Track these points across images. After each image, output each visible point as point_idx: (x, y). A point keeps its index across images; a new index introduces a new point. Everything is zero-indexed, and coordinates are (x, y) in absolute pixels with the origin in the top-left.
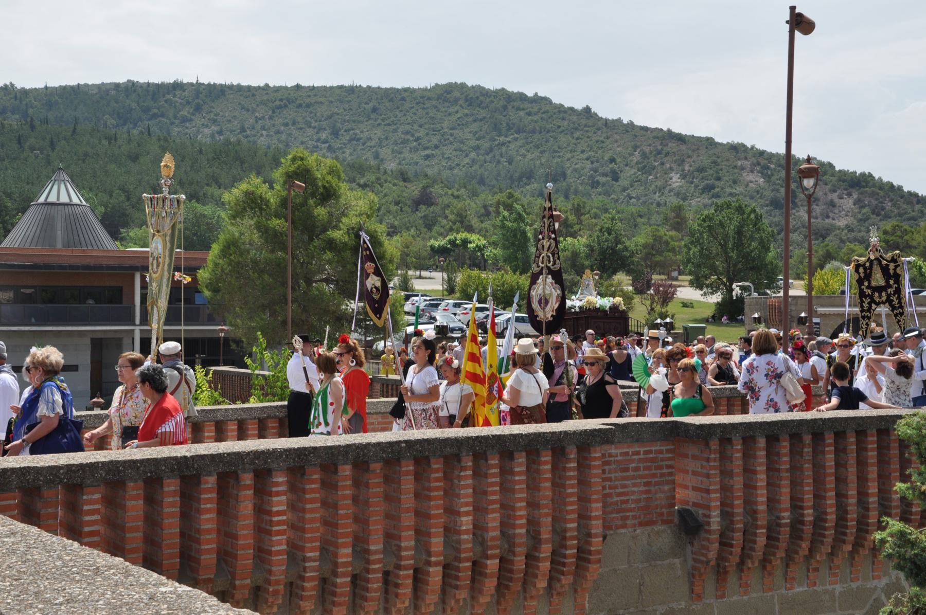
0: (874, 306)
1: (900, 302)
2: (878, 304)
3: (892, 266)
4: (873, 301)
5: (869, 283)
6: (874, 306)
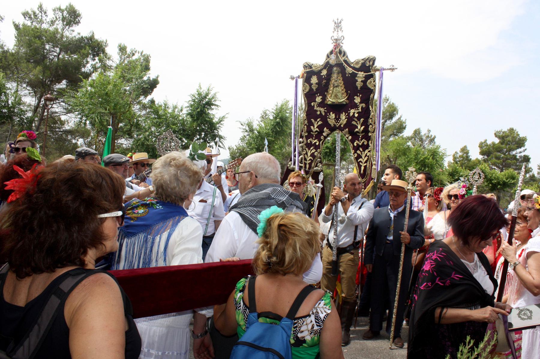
0: (326, 131)
1: (366, 131)
2: (332, 129)
3: (361, 75)
4: (325, 124)
5: (324, 98)
6: (326, 131)
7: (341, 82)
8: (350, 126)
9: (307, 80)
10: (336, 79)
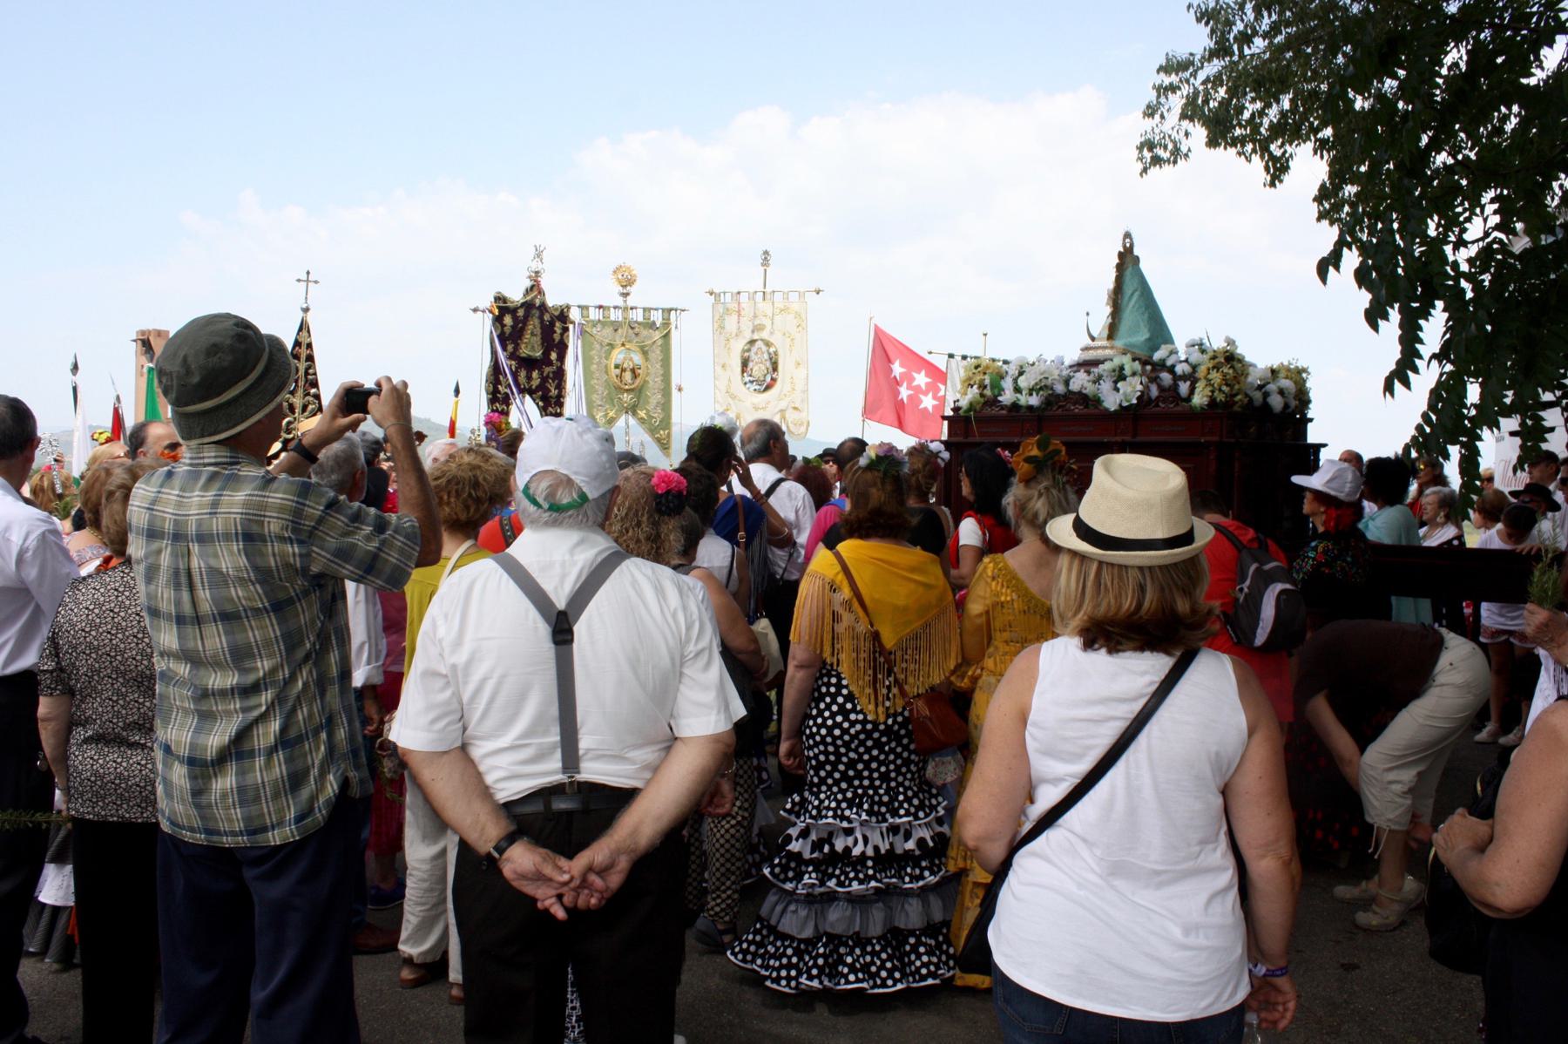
5: (517, 347)
7: (538, 331)
8: (542, 387)
9: (498, 320)
10: (534, 325)
